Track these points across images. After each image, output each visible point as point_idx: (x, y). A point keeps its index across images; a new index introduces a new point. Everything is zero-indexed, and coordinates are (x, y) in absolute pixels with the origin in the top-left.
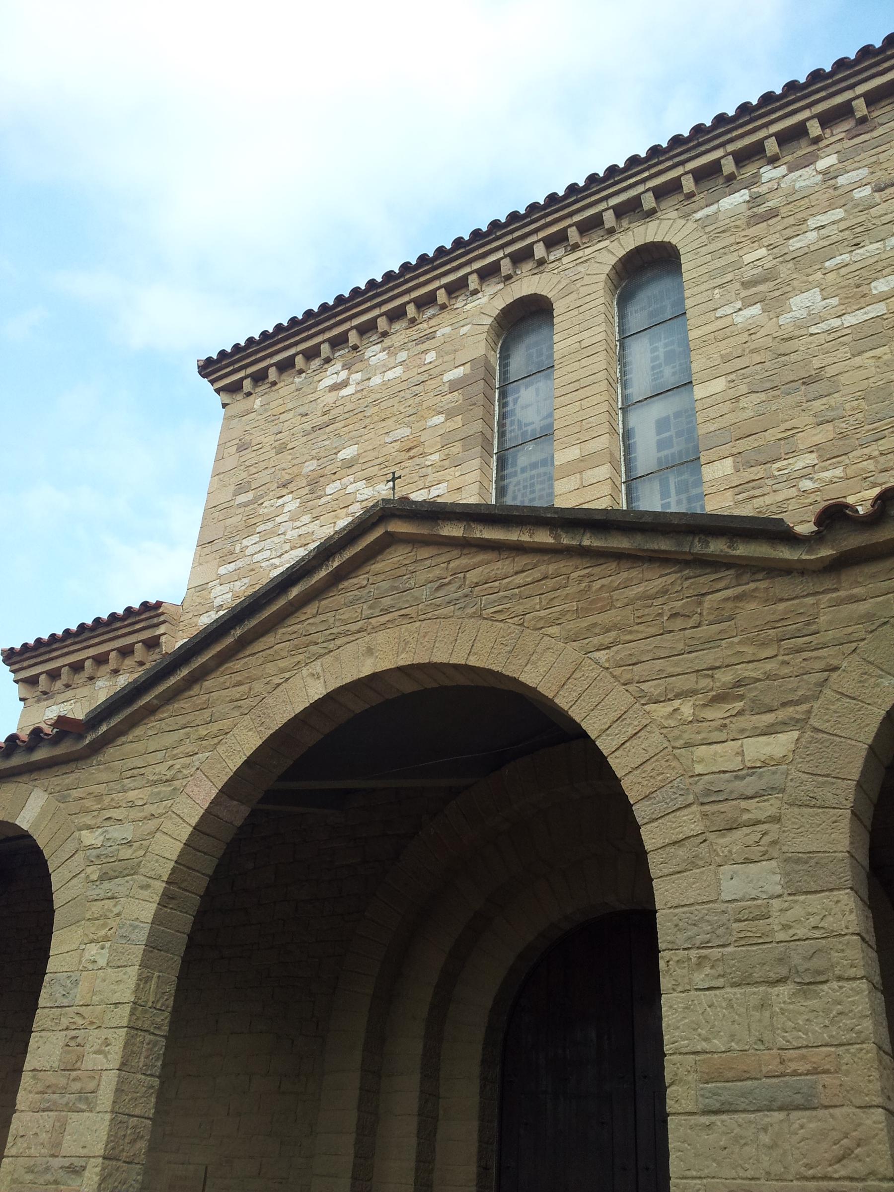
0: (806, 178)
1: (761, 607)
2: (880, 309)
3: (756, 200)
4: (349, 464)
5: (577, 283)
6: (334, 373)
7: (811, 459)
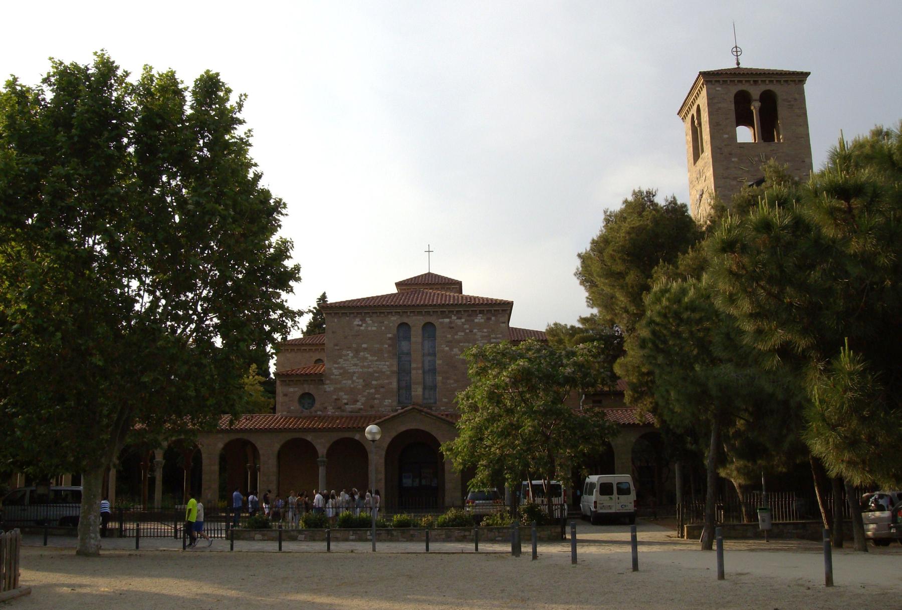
0: (459, 322)
3: (450, 322)
4: (365, 349)
5: (416, 322)
6: (357, 322)
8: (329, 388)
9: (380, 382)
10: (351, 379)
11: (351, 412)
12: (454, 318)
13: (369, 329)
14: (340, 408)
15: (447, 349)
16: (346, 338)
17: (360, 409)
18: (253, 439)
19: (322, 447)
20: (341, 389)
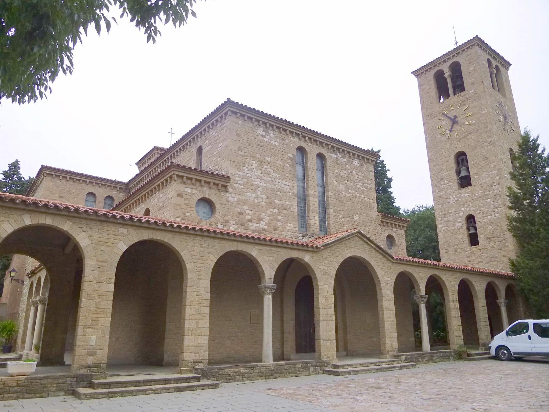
1: (389, 264)
2: (349, 195)
3: (337, 158)
6: (261, 131)
7: (341, 216)
8: (232, 197)
9: (282, 202)
10: (255, 191)
11: (254, 231)
12: (339, 155)
13: (272, 142)
14: (242, 225)
15: (336, 183)
16: (250, 144)
17: (264, 230)
18: (177, 243)
19: (269, 264)
20: (244, 202)
